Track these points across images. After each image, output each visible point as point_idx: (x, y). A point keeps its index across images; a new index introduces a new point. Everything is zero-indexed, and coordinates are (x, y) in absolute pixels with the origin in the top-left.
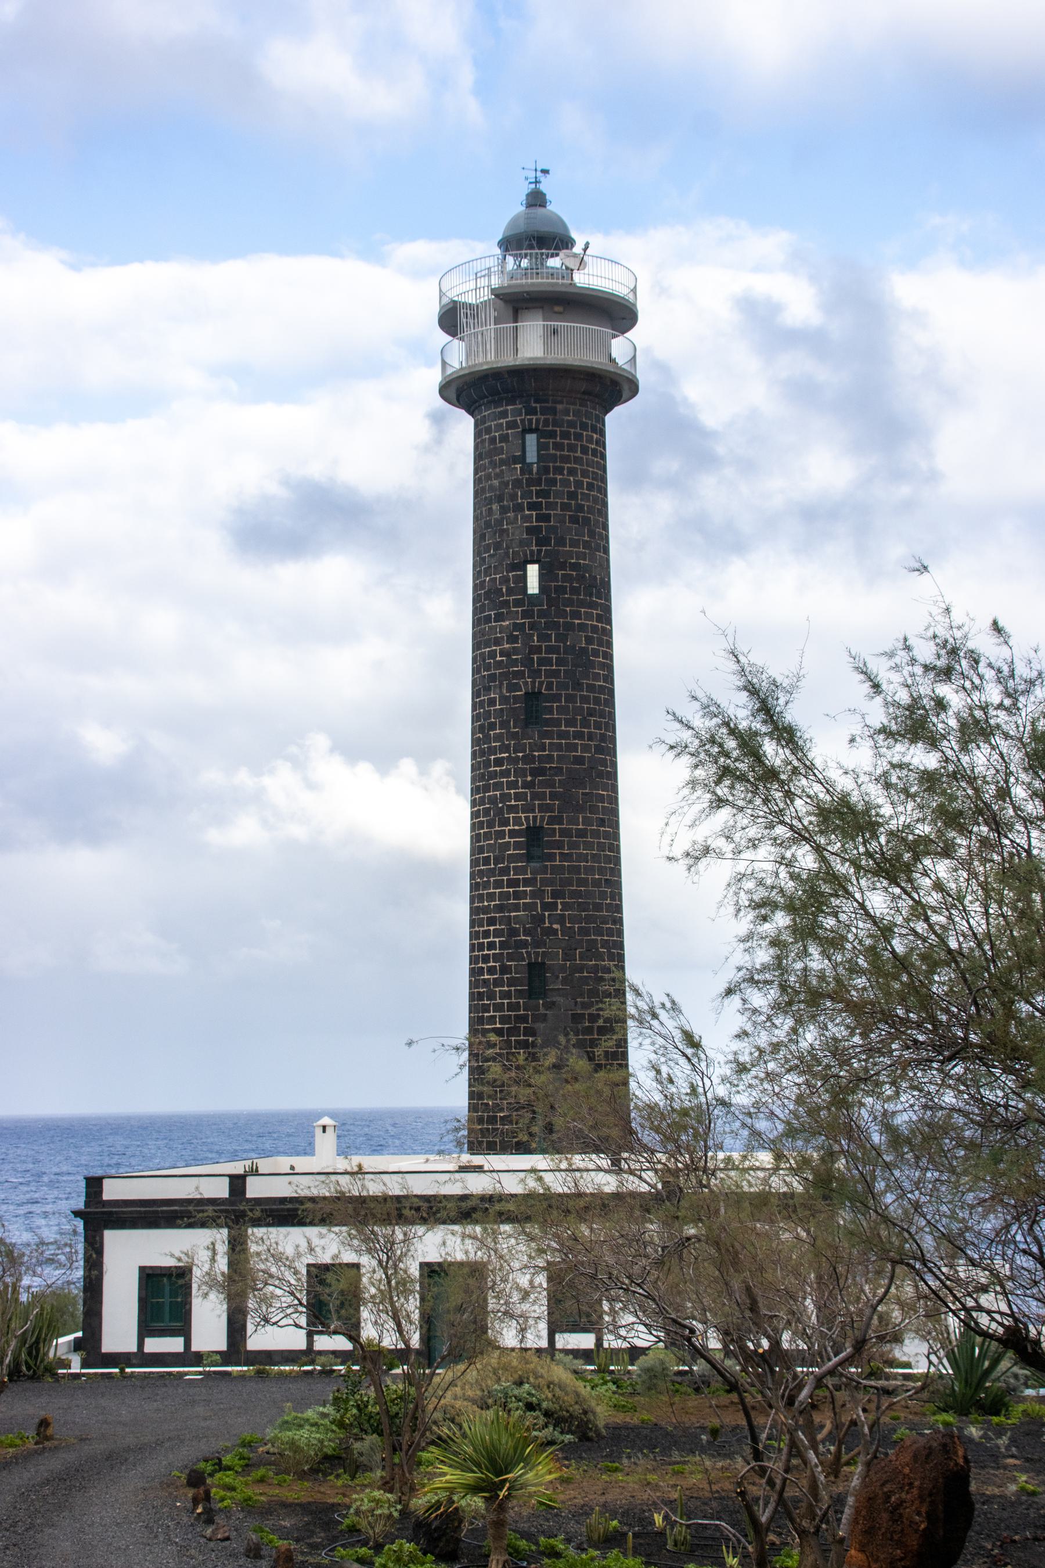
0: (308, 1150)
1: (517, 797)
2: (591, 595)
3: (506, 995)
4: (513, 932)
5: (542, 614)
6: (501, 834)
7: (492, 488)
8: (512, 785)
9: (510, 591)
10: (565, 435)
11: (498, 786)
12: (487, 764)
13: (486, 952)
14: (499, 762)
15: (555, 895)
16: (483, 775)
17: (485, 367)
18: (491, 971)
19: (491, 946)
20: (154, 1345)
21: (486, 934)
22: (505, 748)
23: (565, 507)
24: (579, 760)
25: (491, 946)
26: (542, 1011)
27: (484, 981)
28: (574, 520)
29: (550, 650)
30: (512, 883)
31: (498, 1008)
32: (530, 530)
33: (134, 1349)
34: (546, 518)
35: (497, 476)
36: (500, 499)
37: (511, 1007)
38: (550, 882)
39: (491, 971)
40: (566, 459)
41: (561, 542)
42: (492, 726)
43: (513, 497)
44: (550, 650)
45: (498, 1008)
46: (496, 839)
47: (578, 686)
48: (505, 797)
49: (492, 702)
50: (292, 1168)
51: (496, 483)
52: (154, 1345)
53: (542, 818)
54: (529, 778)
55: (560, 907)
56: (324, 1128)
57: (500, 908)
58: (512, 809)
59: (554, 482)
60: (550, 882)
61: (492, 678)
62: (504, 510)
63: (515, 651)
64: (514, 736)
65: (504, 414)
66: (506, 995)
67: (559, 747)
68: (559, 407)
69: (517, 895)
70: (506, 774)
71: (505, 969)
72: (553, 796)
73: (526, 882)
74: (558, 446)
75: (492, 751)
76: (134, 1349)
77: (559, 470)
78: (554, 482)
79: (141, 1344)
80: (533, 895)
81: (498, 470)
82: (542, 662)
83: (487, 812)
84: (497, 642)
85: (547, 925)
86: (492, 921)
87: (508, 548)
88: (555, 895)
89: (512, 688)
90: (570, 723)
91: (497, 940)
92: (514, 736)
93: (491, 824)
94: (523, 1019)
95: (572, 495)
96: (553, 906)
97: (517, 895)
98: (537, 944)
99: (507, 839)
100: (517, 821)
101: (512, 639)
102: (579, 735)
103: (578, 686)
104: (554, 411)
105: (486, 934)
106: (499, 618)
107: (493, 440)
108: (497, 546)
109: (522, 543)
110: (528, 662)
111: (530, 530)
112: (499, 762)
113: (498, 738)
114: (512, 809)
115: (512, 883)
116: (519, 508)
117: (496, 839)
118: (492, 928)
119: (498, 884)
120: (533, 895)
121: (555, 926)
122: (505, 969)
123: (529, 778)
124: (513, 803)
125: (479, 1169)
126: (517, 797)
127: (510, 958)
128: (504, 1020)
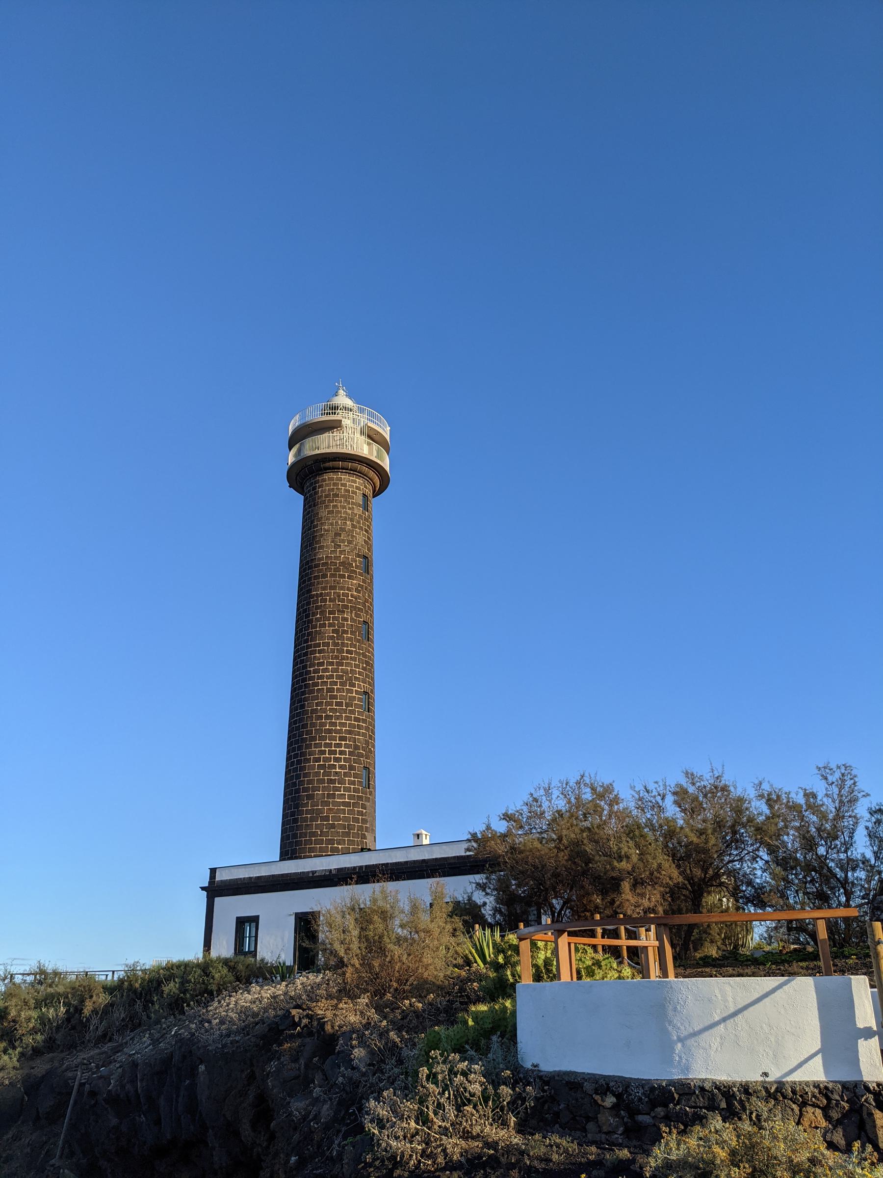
4: (356, 747)
6: (351, 691)
7: (345, 512)
8: (357, 666)
9: (357, 567)
11: (348, 664)
14: (348, 652)
18: (341, 767)
19: (341, 753)
21: (339, 745)
22: (352, 645)
25: (341, 753)
27: (336, 773)
30: (356, 719)
31: (347, 789)
35: (350, 509)
36: (352, 520)
39: (341, 767)
45: (347, 789)
51: (350, 512)
57: (350, 732)
66: (353, 783)
70: (354, 659)
71: (352, 768)
84: (348, 589)
86: (342, 739)
89: (357, 615)
93: (342, 684)
105: (339, 745)
106: (350, 577)
108: (350, 542)
112: (348, 652)
113: (348, 639)
115: (356, 719)
117: (347, 693)
119: (348, 718)
122: (352, 768)
128: (350, 797)
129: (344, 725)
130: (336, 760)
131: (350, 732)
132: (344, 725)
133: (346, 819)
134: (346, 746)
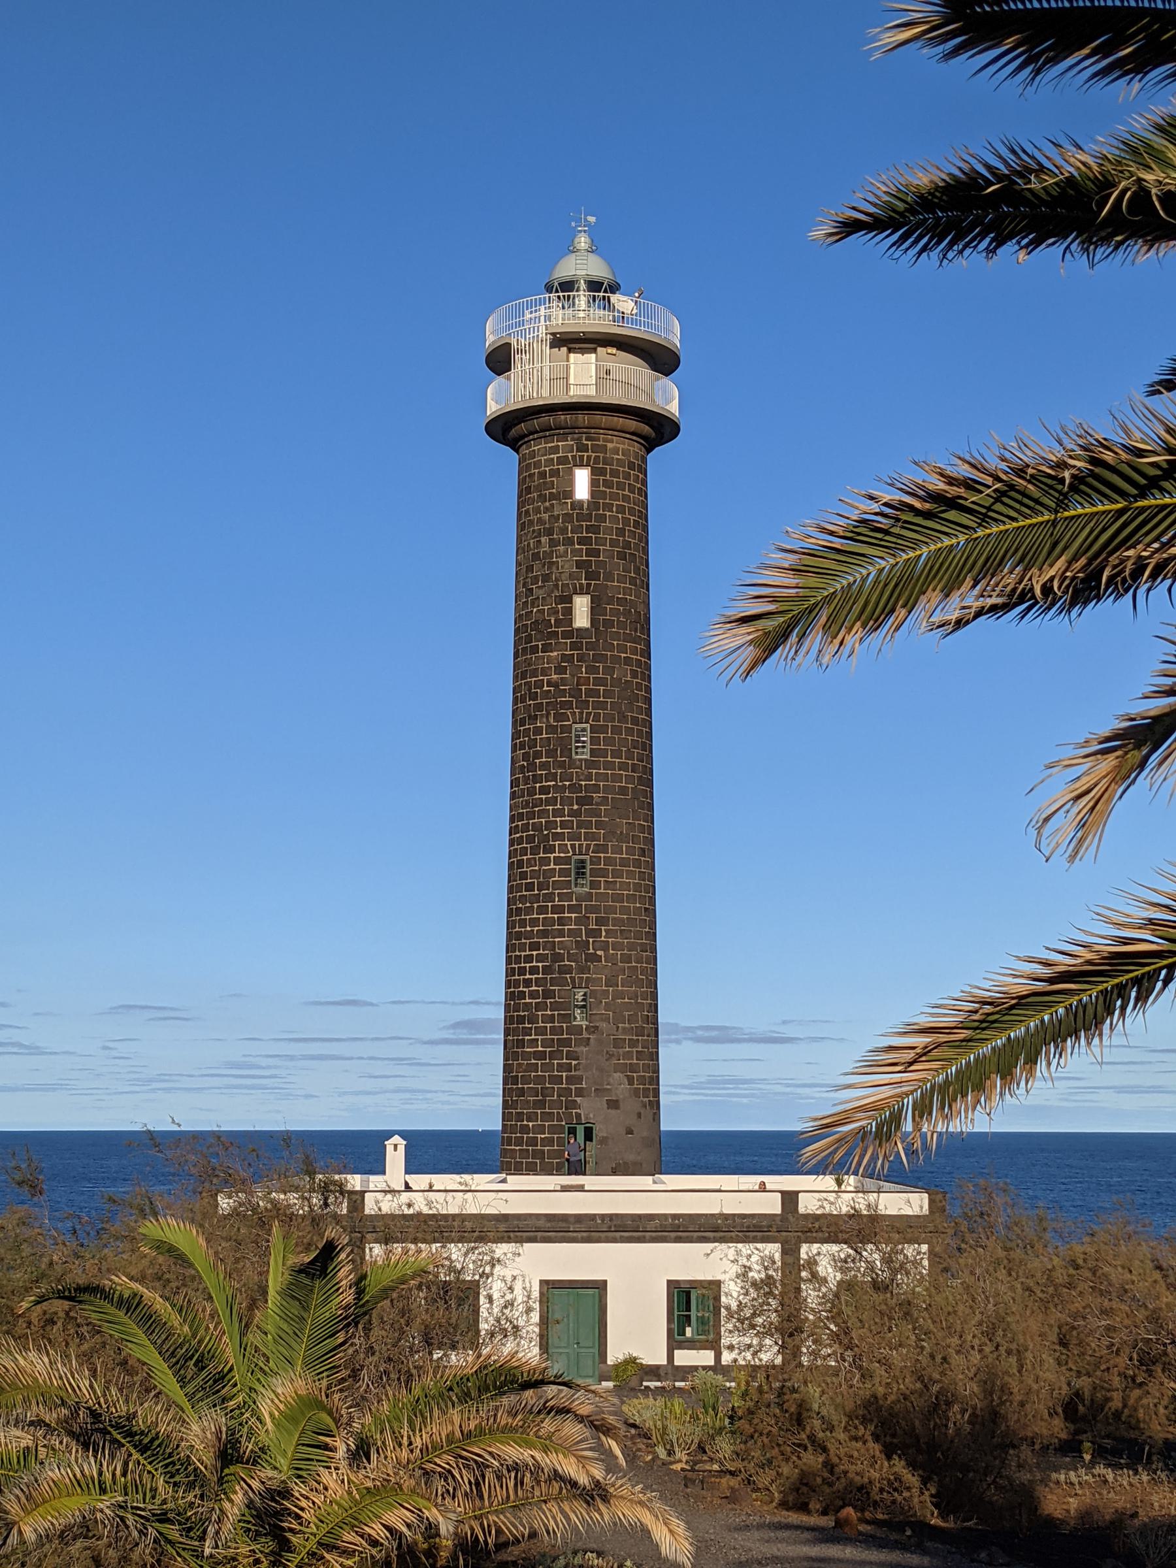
0: (379, 1168)
1: (564, 825)
2: (636, 631)
3: (551, 1019)
4: (557, 958)
5: (591, 646)
6: (546, 861)
7: (540, 521)
8: (556, 813)
10: (615, 473)
12: (531, 792)
13: (528, 976)
15: (599, 921)
16: (527, 802)
17: (541, 403)
18: (533, 995)
20: (684, 1358)
21: (529, 959)
23: (614, 543)
24: (623, 790)
25: (534, 970)
26: (585, 1035)
28: (622, 556)
29: (598, 682)
30: (555, 909)
31: (541, 1031)
32: (579, 564)
33: (662, 1360)
34: (597, 553)
35: (546, 510)
36: (549, 532)
37: (554, 1031)
38: (595, 909)
39: (533, 995)
40: (614, 497)
41: (609, 577)
42: (538, 755)
43: (564, 531)
44: (598, 682)
45: (541, 1031)
46: (541, 865)
47: (623, 718)
48: (550, 825)
49: (538, 731)
50: (431, 1186)
51: (546, 516)
52: (684, 1358)
53: (588, 846)
54: (576, 807)
55: (604, 934)
56: (396, 1146)
57: (544, 934)
58: (557, 836)
59: (602, 518)
60: (595, 909)
61: (539, 707)
62: (553, 543)
63: (563, 681)
64: (562, 765)
65: (555, 450)
66: (551, 1019)
67: (605, 777)
68: (610, 445)
69: (561, 921)
70: (553, 801)
71: (548, 994)
72: (599, 825)
73: (571, 909)
74: (607, 484)
75: (537, 778)
76: (662, 1360)
77: (609, 507)
78: (602, 518)
79: (670, 1357)
80: (578, 921)
81: (547, 504)
82: (590, 693)
83: (530, 839)
85: (591, 951)
87: (557, 580)
88: (599, 921)
90: (617, 754)
91: (540, 964)
92: (562, 765)
93: (535, 851)
94: (567, 1042)
95: (621, 532)
96: (596, 933)
97: (561, 921)
98: (582, 970)
99: (552, 866)
100: (563, 849)
101: (560, 670)
102: (623, 767)
103: (623, 718)
104: (604, 449)
105: (529, 959)
107: (543, 475)
109: (571, 576)
110: (575, 693)
111: (579, 564)
113: (544, 766)
114: (557, 836)
115: (555, 909)
116: (569, 542)
117: (541, 865)
118: (535, 953)
119: (542, 910)
120: (578, 921)
121: (599, 953)
122: (548, 994)
123: (576, 807)
124: (559, 830)
125: (580, 1189)
126: (564, 825)
127: (553, 982)
129: (534, 922)
130: (528, 983)
131: (544, 934)
132: (534, 922)
133: (540, 1080)
134: (540, 958)
